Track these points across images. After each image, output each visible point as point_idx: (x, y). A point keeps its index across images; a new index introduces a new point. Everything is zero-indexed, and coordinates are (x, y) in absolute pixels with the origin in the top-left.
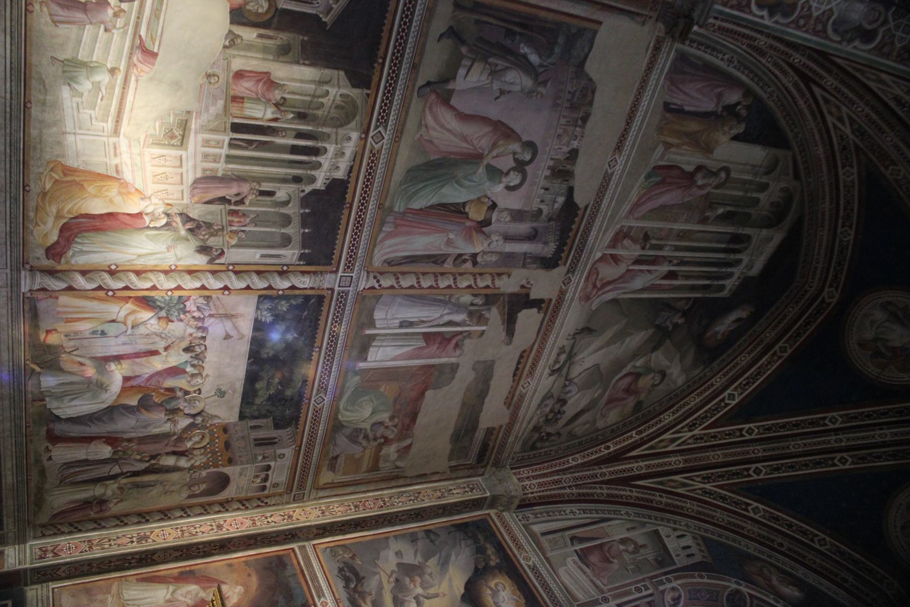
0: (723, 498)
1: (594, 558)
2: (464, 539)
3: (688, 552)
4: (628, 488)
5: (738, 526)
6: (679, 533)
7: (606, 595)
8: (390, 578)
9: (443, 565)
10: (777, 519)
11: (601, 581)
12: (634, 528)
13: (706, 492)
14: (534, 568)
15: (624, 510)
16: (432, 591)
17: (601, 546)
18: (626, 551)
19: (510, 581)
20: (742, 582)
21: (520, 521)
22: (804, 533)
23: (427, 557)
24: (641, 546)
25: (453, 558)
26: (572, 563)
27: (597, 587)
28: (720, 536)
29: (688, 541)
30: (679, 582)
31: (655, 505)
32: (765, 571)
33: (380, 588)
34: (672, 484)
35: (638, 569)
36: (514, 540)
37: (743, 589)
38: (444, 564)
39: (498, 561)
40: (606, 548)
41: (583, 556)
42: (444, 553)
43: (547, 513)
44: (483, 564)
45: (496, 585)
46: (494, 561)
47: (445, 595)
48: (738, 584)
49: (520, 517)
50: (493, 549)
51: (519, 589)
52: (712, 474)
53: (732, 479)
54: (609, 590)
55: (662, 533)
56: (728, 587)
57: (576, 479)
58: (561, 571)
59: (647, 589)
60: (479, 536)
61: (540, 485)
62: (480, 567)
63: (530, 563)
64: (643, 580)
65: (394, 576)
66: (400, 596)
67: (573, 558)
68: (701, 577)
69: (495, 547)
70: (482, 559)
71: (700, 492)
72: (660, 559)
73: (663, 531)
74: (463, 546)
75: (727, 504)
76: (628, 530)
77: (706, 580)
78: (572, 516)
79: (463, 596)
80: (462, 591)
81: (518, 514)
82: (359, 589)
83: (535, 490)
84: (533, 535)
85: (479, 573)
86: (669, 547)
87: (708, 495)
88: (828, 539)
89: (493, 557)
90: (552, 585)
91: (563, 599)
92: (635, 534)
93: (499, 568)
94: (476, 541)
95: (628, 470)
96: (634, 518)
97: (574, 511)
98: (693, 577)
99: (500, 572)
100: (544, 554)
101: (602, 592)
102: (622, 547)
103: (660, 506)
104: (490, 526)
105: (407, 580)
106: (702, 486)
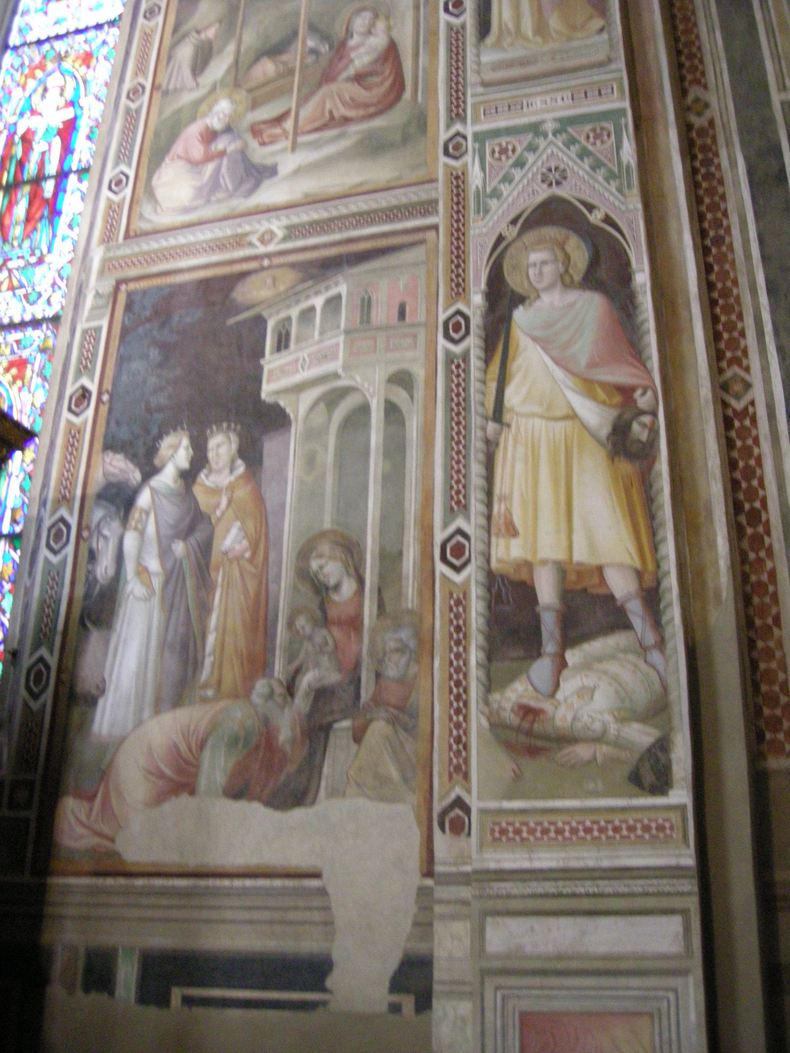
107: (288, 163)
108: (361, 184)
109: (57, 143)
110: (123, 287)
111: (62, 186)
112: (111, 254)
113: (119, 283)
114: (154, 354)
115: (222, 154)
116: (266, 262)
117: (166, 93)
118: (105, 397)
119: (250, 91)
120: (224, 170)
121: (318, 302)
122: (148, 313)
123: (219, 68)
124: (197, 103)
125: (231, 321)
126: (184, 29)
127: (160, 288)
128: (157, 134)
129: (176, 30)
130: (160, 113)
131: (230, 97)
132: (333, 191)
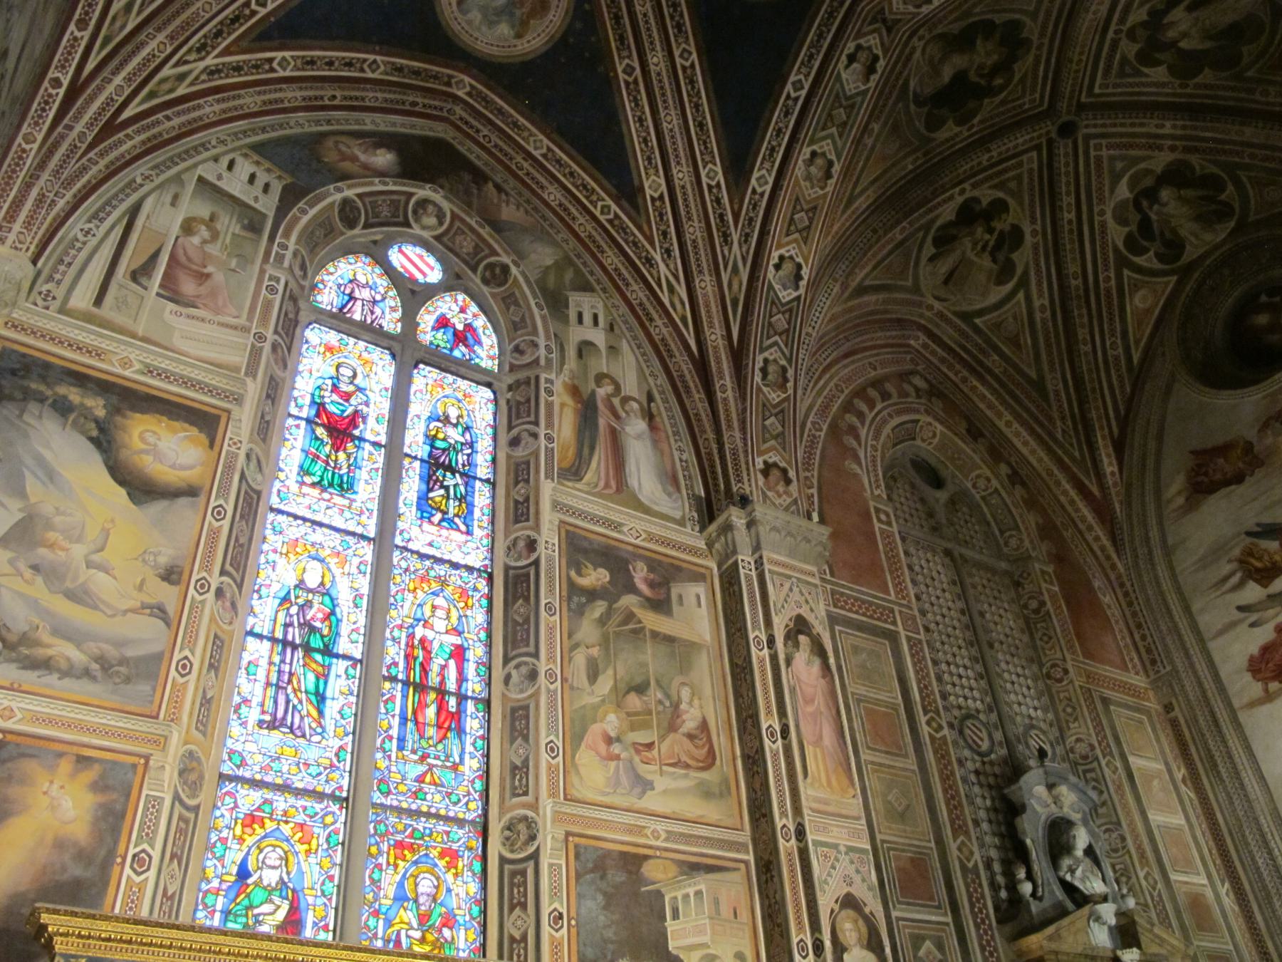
0: (238, 69)
1: (188, 287)
2: (22, 411)
3: (260, 182)
4: (121, 135)
5: (276, 101)
6: (225, 162)
7: (253, 331)
8: (22, 576)
9: (51, 479)
10: (311, 62)
11: (229, 315)
12: (176, 197)
13: (212, 73)
14: (150, 371)
15: (137, 172)
16: (92, 533)
17: (173, 257)
18: (205, 242)
19: (146, 417)
20: (339, 184)
21: (47, 308)
22: (349, 64)
23: (21, 494)
24: (213, 218)
25: (48, 455)
26: (173, 317)
27: (236, 328)
28: (264, 130)
29: (245, 168)
30: (294, 238)
31: (166, 136)
32: (344, 149)
33: (34, 604)
34: (166, 86)
35: (245, 260)
36: (90, 352)
37: (350, 193)
38: (51, 476)
39: (101, 402)
40: (183, 259)
41: (171, 292)
42: (29, 460)
43: (61, 261)
44: (93, 425)
45: (142, 439)
46: (98, 407)
47: (113, 521)
48: (339, 190)
49: (40, 302)
50: (73, 389)
51: (170, 419)
52: (205, 36)
53: (235, 30)
54: (250, 318)
55: (211, 178)
56: (333, 203)
57: (56, 173)
58: (178, 342)
59: (278, 281)
60: (34, 386)
61: (28, 224)
62: (95, 433)
63: (137, 366)
64: (262, 272)
65: (21, 565)
66: (69, 584)
67: (168, 310)
68: (304, 212)
69: (72, 385)
70: (82, 420)
71: (204, 77)
72: (246, 222)
73: (208, 171)
74: (32, 421)
75: (246, 74)
76: (173, 204)
77: (313, 212)
78: (93, 242)
79: (129, 494)
80: (122, 492)
81: (31, 299)
82: (12, 638)
83: (29, 239)
84: (88, 318)
85: (105, 444)
86: (236, 193)
87: (216, 76)
88: (379, 58)
89: (90, 402)
90: (195, 374)
91: (225, 381)
92: (186, 206)
93: (115, 411)
94: (42, 400)
95: (108, 104)
96: (163, 177)
97: (87, 226)
98: (296, 220)
99: (124, 416)
100: (134, 336)
101: (245, 330)
102: (196, 240)
103: (174, 134)
104: (24, 355)
105: (42, 551)
106: (202, 65)
107: (661, 783)
108: (702, 817)
109: (452, 663)
110: (571, 839)
111: (462, 708)
112: (557, 808)
113: (568, 834)
114: (600, 898)
115: (618, 757)
116: (658, 853)
117: (572, 688)
118: (573, 922)
119: (629, 714)
120: (621, 772)
121: (691, 891)
122: (590, 865)
123: (605, 684)
124: (595, 708)
125: (643, 889)
126: (579, 636)
127: (596, 849)
128: (572, 720)
129: (570, 636)
130: (571, 703)
131: (615, 712)
132: (689, 816)
